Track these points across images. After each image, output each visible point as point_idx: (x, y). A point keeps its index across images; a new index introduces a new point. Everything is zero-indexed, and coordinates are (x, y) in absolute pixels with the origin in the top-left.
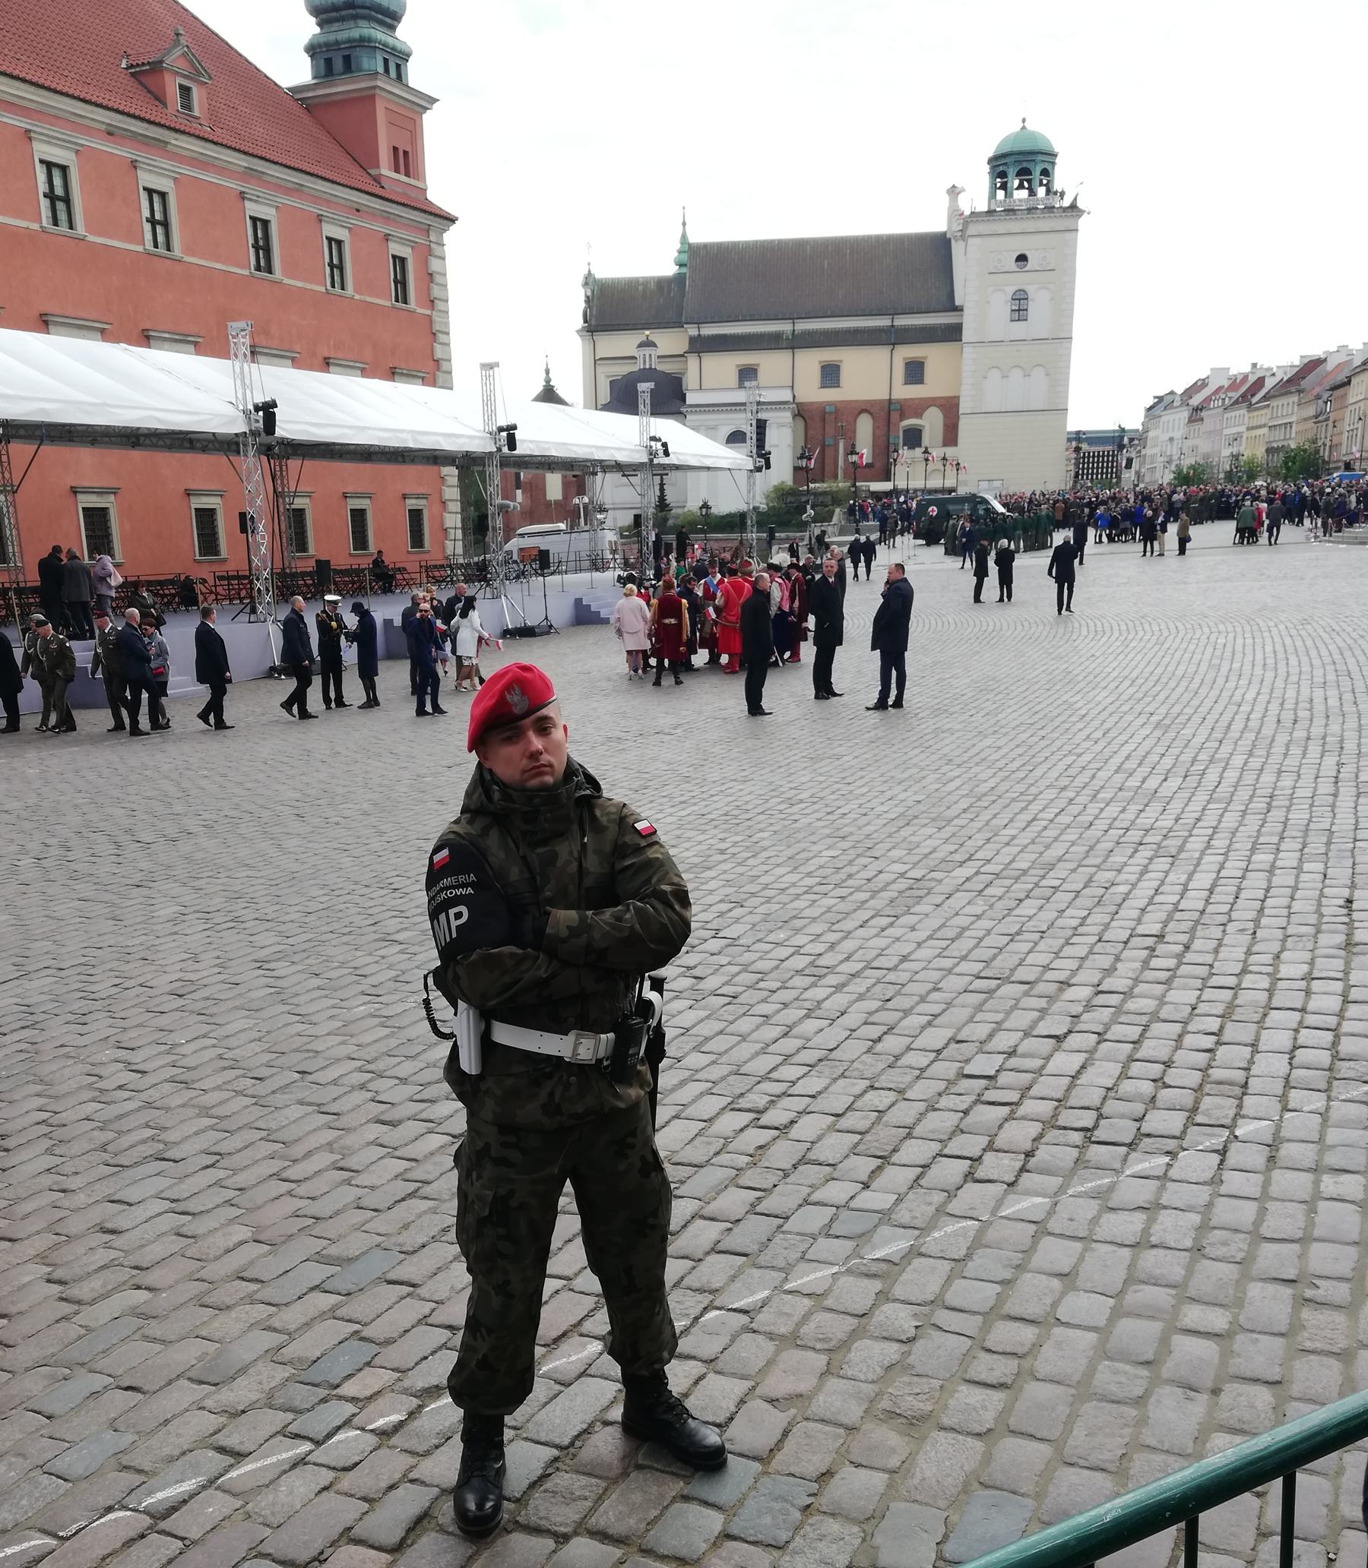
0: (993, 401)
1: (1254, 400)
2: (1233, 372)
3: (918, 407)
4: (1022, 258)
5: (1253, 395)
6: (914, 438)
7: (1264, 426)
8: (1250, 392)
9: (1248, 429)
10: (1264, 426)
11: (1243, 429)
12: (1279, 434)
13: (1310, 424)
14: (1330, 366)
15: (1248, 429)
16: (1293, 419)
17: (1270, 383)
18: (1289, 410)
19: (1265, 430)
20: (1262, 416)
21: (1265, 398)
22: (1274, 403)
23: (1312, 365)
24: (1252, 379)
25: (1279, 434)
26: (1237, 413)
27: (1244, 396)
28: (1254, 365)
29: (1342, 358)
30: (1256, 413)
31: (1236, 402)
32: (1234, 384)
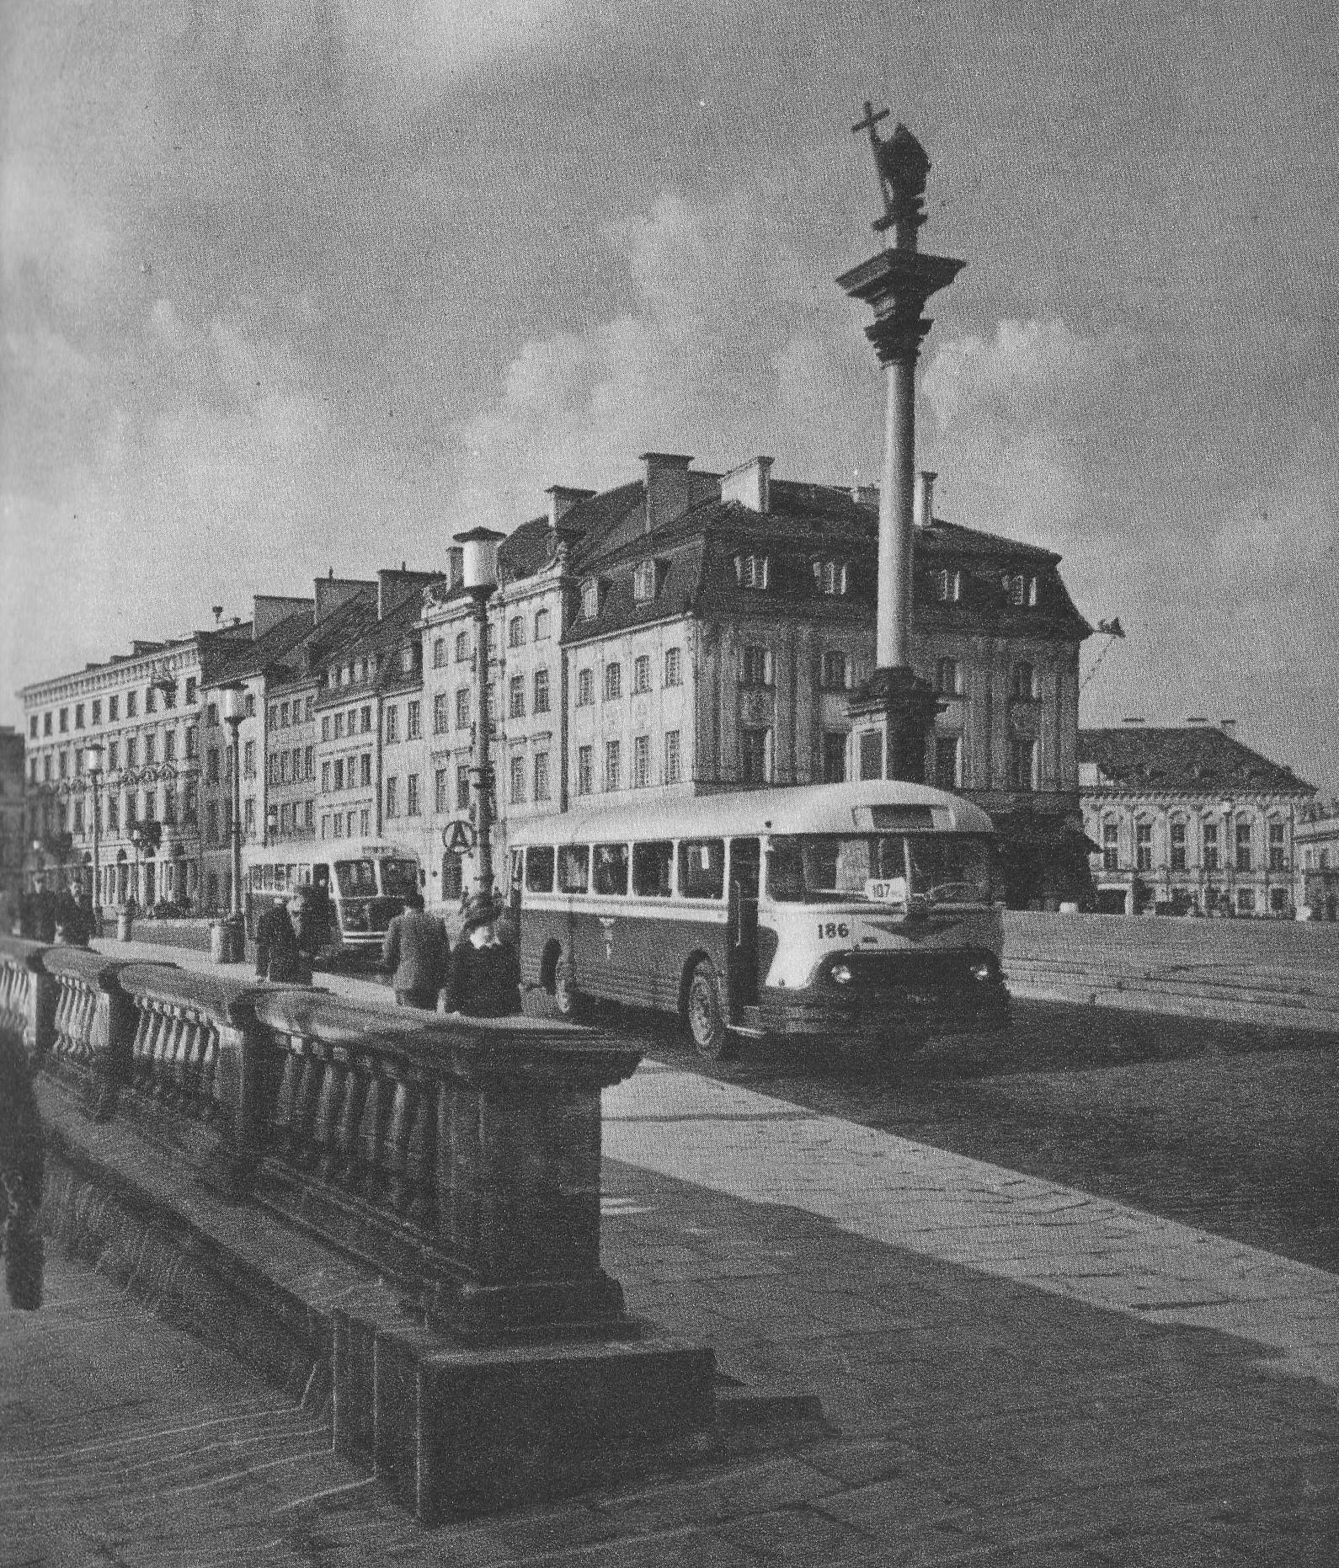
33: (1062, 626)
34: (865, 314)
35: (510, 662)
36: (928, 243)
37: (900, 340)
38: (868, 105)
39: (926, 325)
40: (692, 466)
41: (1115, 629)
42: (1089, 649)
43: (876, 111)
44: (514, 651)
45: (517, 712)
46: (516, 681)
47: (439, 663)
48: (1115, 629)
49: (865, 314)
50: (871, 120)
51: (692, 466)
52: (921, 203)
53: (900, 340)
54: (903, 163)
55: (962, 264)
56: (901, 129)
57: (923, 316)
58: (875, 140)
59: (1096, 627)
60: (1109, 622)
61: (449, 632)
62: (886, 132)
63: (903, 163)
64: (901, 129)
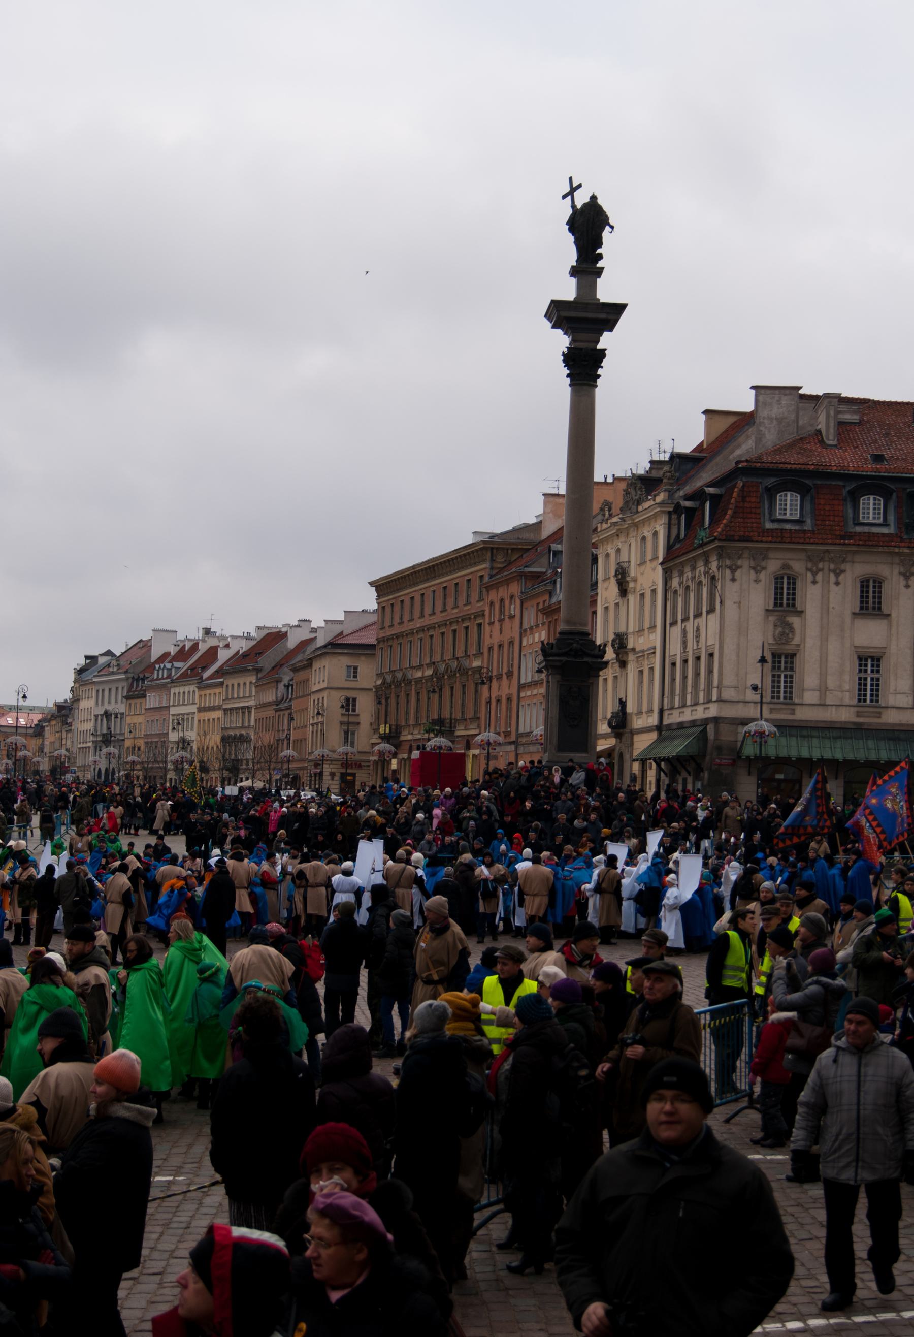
1: (206, 674)
2: (181, 636)
5: (204, 668)
7: (218, 708)
8: (196, 662)
9: (200, 710)
10: (218, 708)
11: (193, 709)
12: (236, 721)
13: (270, 712)
14: (292, 642)
15: (200, 710)
16: (252, 703)
17: (223, 656)
18: (245, 691)
19: (219, 714)
20: (215, 697)
21: (220, 673)
22: (231, 681)
23: (275, 637)
24: (203, 648)
25: (236, 721)
26: (187, 689)
27: (192, 668)
29: (305, 635)
30: (208, 692)
31: (184, 675)
32: (183, 654)
34: (561, 341)
35: (640, 580)
37: (584, 366)
38: (571, 179)
40: (801, 392)
43: (575, 185)
44: (643, 568)
49: (561, 341)
51: (801, 392)
52: (600, 257)
53: (584, 366)
54: (588, 225)
56: (594, 198)
57: (599, 347)
58: (573, 206)
62: (581, 198)
63: (588, 225)
64: (594, 198)
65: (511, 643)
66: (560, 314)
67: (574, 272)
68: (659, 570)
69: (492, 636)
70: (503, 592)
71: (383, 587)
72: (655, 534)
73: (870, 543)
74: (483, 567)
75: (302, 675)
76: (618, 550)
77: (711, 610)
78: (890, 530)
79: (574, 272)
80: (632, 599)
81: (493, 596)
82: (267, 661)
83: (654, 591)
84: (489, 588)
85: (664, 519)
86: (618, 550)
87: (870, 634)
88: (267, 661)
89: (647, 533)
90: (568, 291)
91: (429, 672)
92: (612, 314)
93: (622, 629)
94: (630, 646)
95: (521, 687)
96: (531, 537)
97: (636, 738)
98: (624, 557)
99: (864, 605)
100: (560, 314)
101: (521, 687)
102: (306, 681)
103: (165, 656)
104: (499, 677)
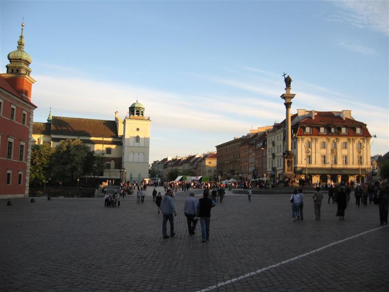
0: (131, 160)
1: (180, 163)
3: (110, 159)
4: (138, 129)
6: (109, 166)
22: (184, 165)
28: (176, 157)
33: (366, 135)
34: (284, 101)
36: (292, 92)
37: (288, 105)
39: (291, 103)
41: (375, 136)
42: (372, 140)
45: (278, 152)
46: (278, 147)
47: (269, 144)
48: (375, 136)
50: (284, 75)
53: (288, 105)
54: (288, 81)
55: (295, 95)
56: (288, 76)
59: (372, 135)
60: (374, 135)
61: (270, 139)
62: (286, 76)
63: (288, 81)
64: (288, 76)
65: (247, 156)
66: (283, 97)
67: (286, 89)
68: (282, 142)
69: (242, 155)
70: (244, 147)
71: (218, 147)
72: (281, 135)
73: (322, 135)
74: (240, 143)
75: (199, 163)
76: (272, 139)
77: (295, 148)
78: (326, 133)
79: (286, 89)
80: (276, 147)
81: (242, 147)
82: (191, 161)
83: (281, 146)
84: (241, 147)
85: (282, 133)
86: (272, 139)
87: (324, 151)
88: (191, 161)
89: (279, 135)
90: (284, 92)
91: (229, 162)
92: (293, 96)
93: (273, 152)
94: (276, 155)
95: (249, 164)
96: (248, 137)
97: (277, 171)
98: (273, 140)
99: (322, 146)
100: (283, 97)
101: (249, 164)
102: (200, 165)
103: (170, 161)
104: (244, 162)
